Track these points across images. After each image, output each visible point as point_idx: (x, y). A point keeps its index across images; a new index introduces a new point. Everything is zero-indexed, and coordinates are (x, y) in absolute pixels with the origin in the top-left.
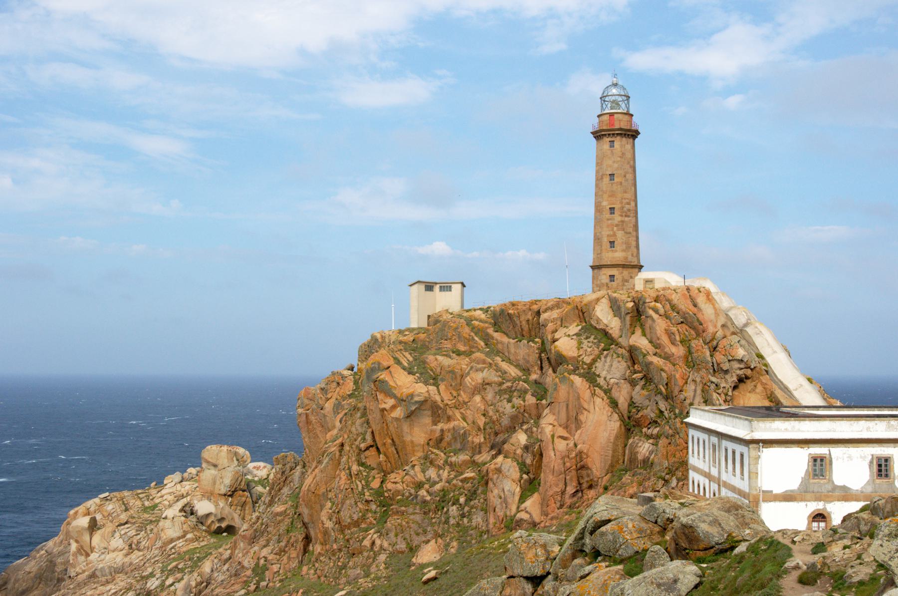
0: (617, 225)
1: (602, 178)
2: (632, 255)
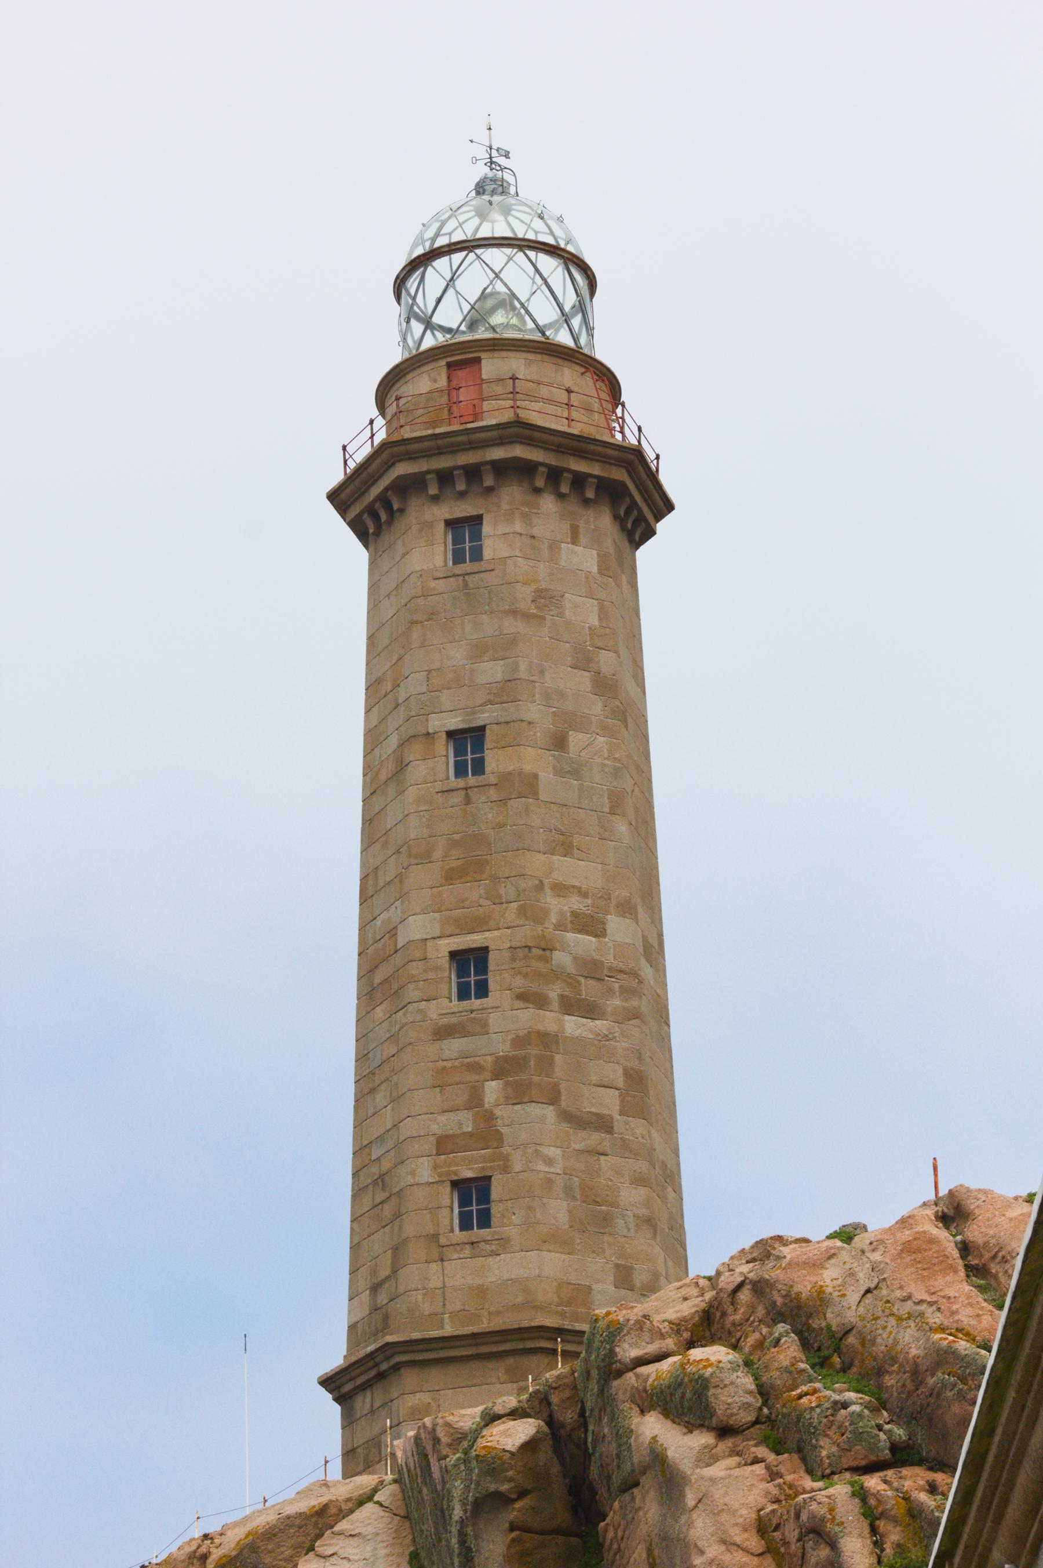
0: (503, 1068)
1: (401, 767)
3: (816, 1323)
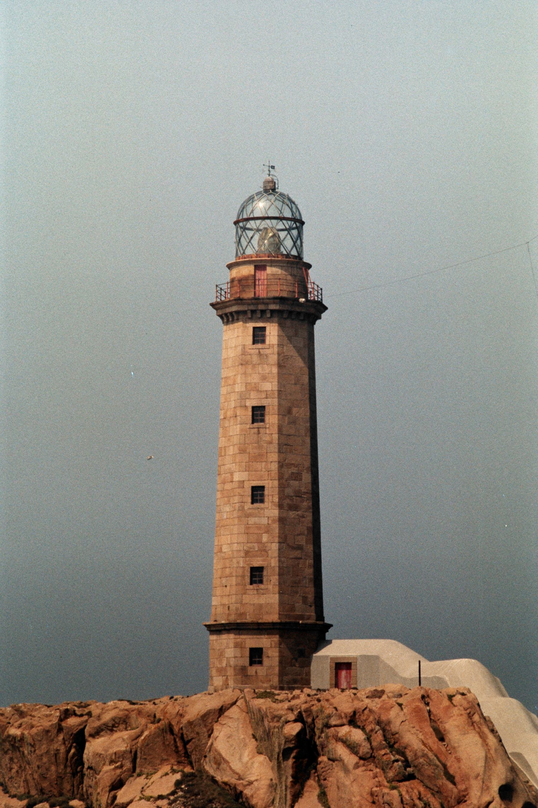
2: (305, 599)
3: (388, 728)
